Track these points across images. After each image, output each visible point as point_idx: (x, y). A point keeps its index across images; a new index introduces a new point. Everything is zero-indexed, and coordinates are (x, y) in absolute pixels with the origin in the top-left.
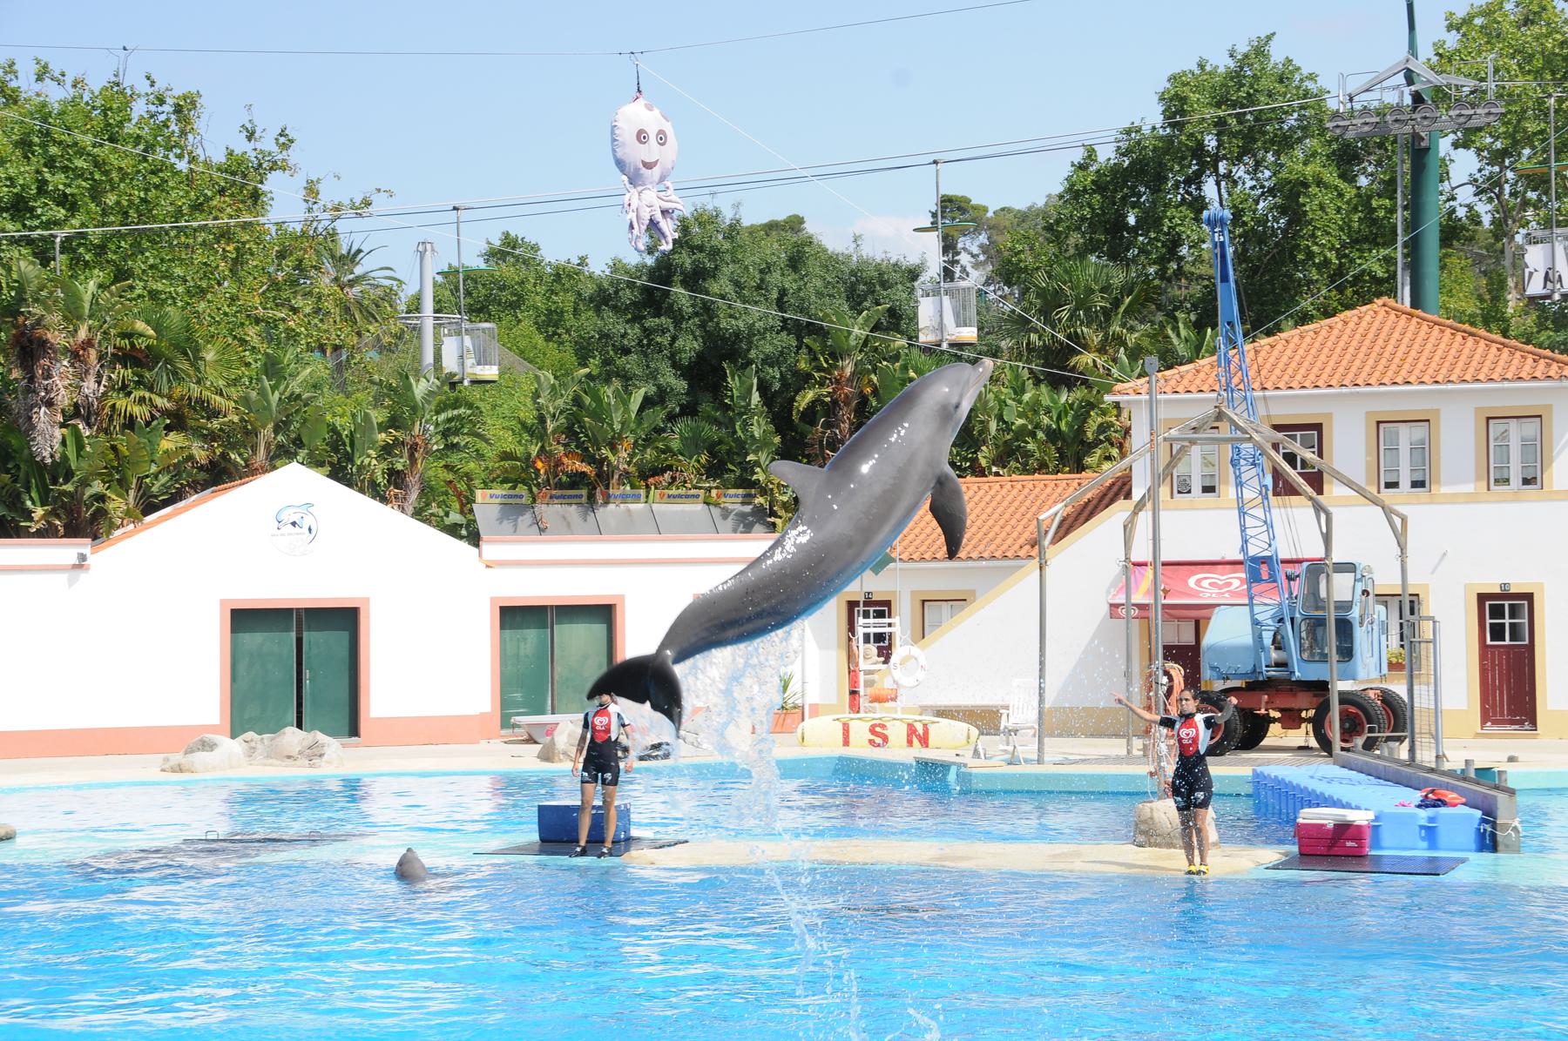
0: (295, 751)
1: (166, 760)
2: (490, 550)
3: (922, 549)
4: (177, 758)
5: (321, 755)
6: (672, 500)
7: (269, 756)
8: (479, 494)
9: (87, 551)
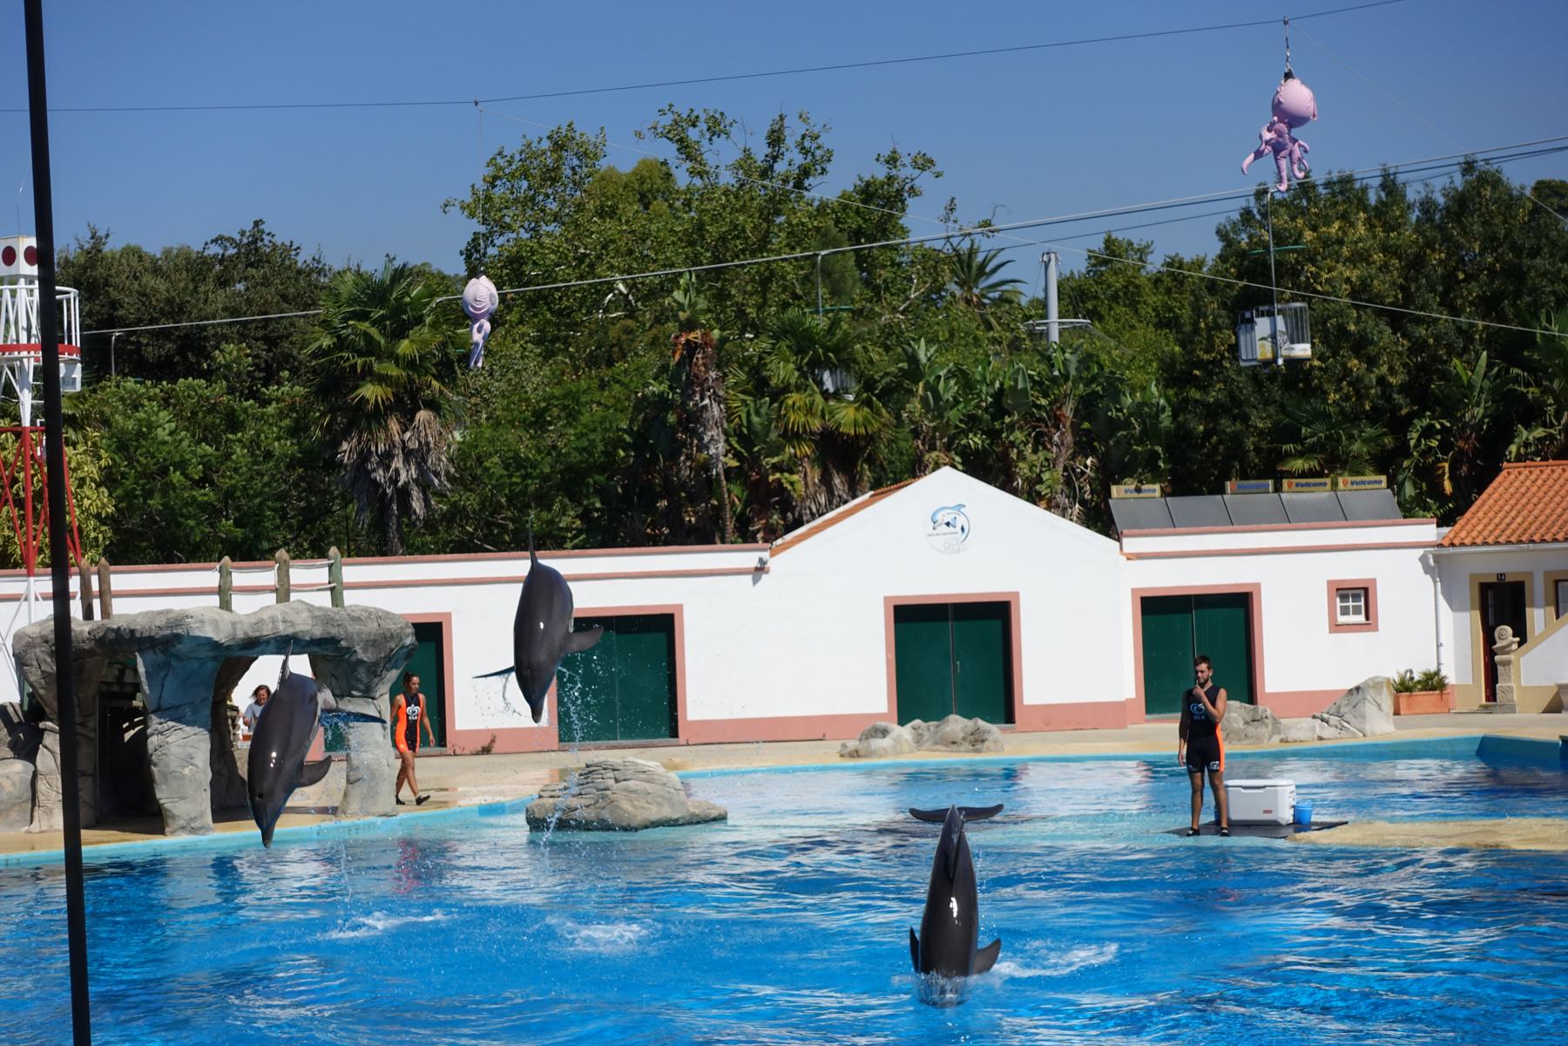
0: (959, 739)
1: (844, 746)
2: (1132, 544)
3: (1554, 530)
4: (852, 744)
5: (983, 741)
6: (1300, 489)
7: (936, 743)
8: (1114, 489)
9: (766, 555)
